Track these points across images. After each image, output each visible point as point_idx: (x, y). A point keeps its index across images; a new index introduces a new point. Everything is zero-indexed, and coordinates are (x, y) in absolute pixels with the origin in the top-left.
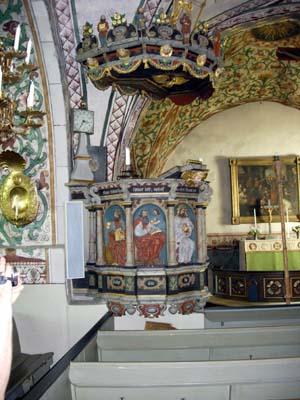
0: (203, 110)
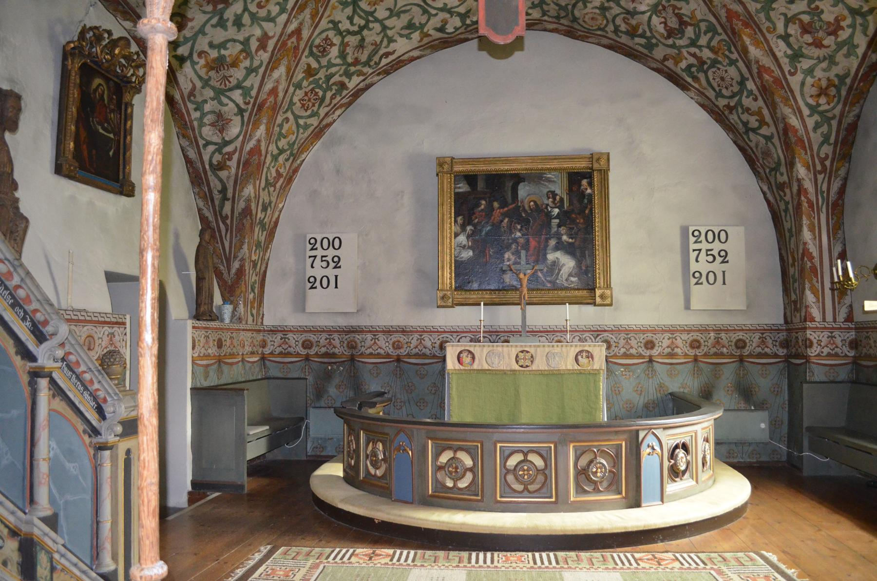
0: (377, 46)
